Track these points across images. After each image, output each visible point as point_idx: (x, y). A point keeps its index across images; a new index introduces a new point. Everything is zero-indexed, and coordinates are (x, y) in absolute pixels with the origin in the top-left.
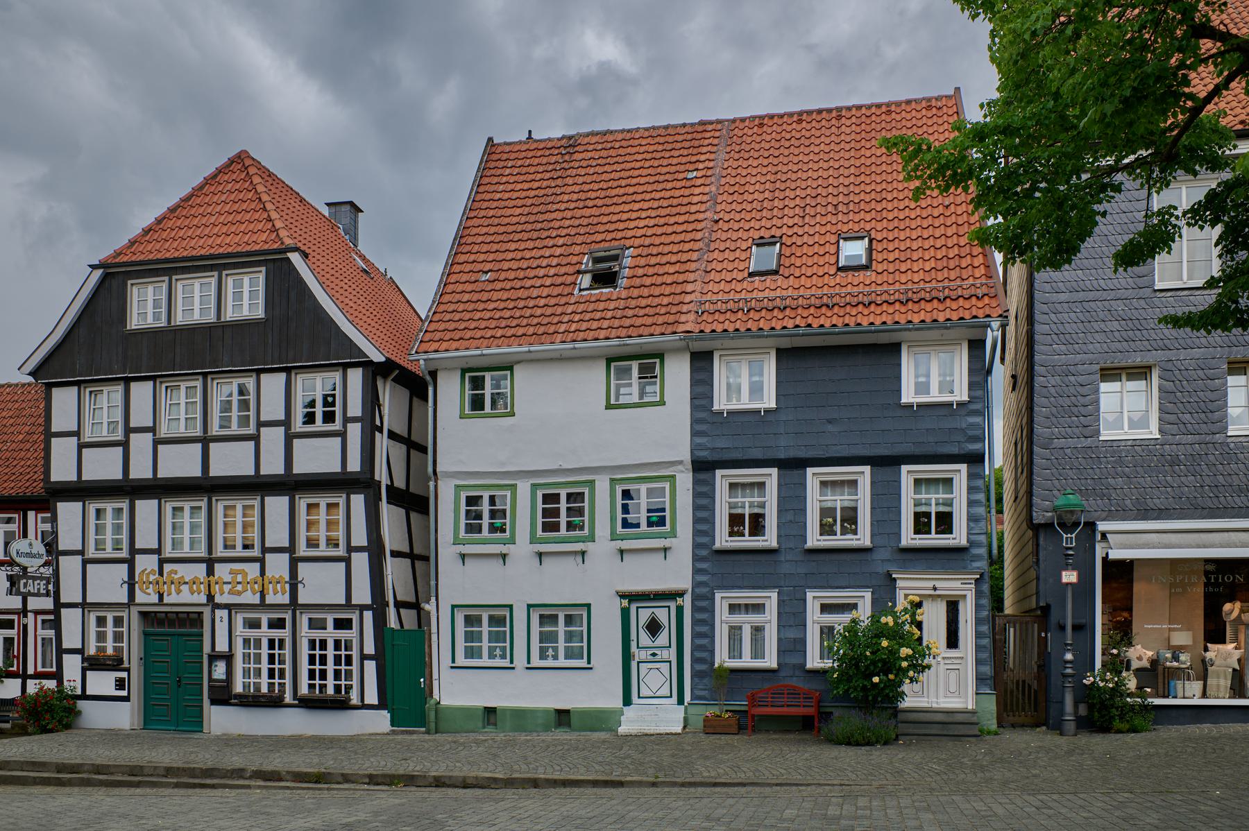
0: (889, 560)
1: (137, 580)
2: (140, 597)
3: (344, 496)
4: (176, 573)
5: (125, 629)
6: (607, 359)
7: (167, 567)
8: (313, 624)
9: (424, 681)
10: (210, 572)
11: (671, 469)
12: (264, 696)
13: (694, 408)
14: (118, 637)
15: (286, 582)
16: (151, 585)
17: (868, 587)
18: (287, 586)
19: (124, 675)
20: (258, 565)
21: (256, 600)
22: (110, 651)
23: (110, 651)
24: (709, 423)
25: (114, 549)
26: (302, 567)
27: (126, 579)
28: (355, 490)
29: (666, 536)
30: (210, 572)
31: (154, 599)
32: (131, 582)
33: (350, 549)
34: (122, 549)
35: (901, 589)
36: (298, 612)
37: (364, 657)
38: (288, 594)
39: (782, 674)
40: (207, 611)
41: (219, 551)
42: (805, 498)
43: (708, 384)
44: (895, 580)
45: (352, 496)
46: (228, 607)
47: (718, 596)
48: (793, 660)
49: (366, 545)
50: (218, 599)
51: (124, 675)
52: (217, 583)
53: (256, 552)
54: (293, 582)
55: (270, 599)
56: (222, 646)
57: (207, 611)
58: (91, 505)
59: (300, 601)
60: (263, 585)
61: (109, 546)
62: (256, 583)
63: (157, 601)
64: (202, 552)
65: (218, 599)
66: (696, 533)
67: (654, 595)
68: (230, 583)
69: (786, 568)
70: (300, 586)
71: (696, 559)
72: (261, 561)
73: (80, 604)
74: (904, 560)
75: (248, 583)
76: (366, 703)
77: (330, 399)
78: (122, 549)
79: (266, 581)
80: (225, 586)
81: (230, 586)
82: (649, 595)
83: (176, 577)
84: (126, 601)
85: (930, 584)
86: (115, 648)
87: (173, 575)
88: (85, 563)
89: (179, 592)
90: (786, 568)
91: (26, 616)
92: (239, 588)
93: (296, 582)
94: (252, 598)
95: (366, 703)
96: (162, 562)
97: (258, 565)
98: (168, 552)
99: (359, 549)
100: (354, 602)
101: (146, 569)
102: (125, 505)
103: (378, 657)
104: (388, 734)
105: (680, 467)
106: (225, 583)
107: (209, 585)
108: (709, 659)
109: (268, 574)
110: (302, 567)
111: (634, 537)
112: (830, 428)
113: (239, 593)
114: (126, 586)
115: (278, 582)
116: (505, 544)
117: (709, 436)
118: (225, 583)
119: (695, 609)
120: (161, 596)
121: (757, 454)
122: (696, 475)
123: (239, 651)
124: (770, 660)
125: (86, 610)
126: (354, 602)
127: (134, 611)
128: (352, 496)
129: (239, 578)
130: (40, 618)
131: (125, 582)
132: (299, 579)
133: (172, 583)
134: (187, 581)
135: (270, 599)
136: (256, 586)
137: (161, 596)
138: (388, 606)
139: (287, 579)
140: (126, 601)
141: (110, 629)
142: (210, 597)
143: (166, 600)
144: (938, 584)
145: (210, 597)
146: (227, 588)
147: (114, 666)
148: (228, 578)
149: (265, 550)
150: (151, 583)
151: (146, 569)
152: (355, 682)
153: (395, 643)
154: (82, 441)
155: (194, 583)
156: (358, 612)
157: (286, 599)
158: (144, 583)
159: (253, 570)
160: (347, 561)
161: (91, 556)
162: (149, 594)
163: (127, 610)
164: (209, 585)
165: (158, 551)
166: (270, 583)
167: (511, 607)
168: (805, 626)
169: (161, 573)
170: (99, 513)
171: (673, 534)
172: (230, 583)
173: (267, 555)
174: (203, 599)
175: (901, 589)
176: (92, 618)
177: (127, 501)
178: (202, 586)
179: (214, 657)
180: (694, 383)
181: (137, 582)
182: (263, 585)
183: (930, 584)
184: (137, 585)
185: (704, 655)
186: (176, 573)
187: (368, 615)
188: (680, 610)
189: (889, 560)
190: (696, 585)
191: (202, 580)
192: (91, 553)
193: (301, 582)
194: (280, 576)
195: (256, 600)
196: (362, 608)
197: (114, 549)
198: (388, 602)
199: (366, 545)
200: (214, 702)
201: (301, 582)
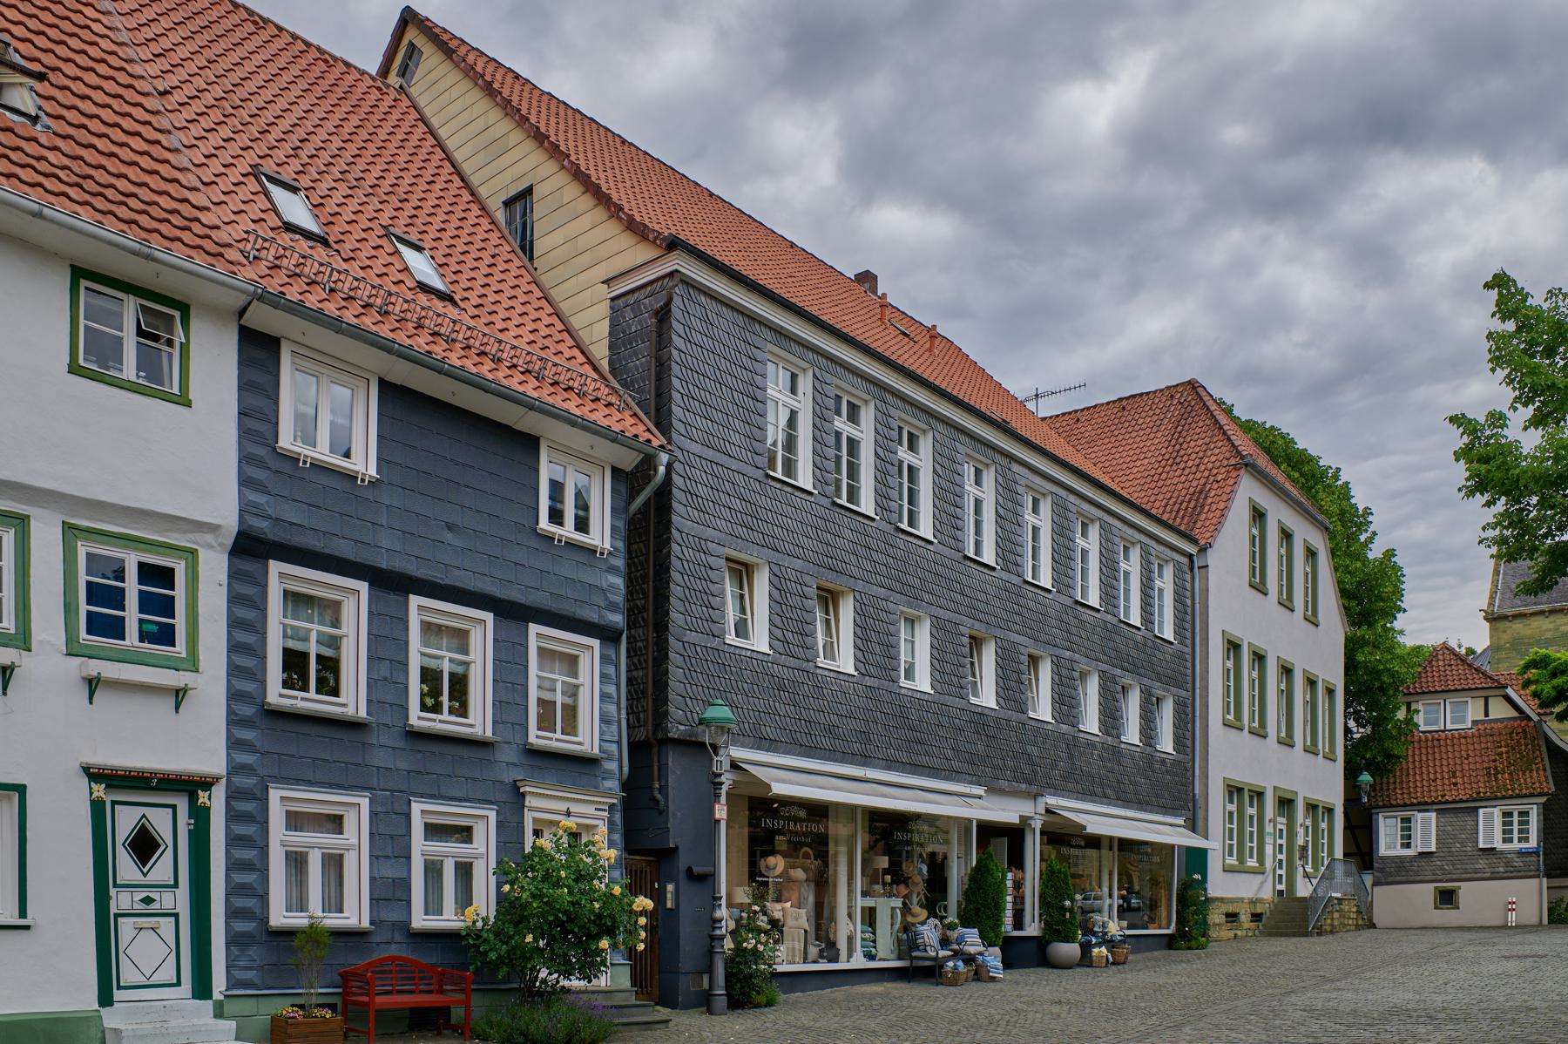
0: (514, 765)
6: (72, 266)
11: (190, 536)
13: (245, 434)
17: (492, 803)
24: (269, 468)
29: (178, 665)
35: (531, 809)
39: (376, 938)
42: (407, 643)
43: (269, 397)
44: (523, 795)
47: (275, 795)
48: (393, 915)
66: (234, 671)
67: (161, 780)
69: (379, 758)
71: (233, 720)
74: (532, 767)
82: (148, 780)
85: (562, 806)
90: (379, 758)
105: (209, 538)
108: (258, 911)
111: (116, 656)
112: (448, 536)
117: (268, 493)
119: (232, 816)
121: (345, 550)
122: (237, 561)
124: (355, 914)
144: (574, 808)
168: (409, 858)
171: (192, 663)
175: (531, 809)
180: (245, 386)
183: (562, 806)
185: (250, 903)
188: (200, 816)
189: (514, 765)
190: (234, 769)
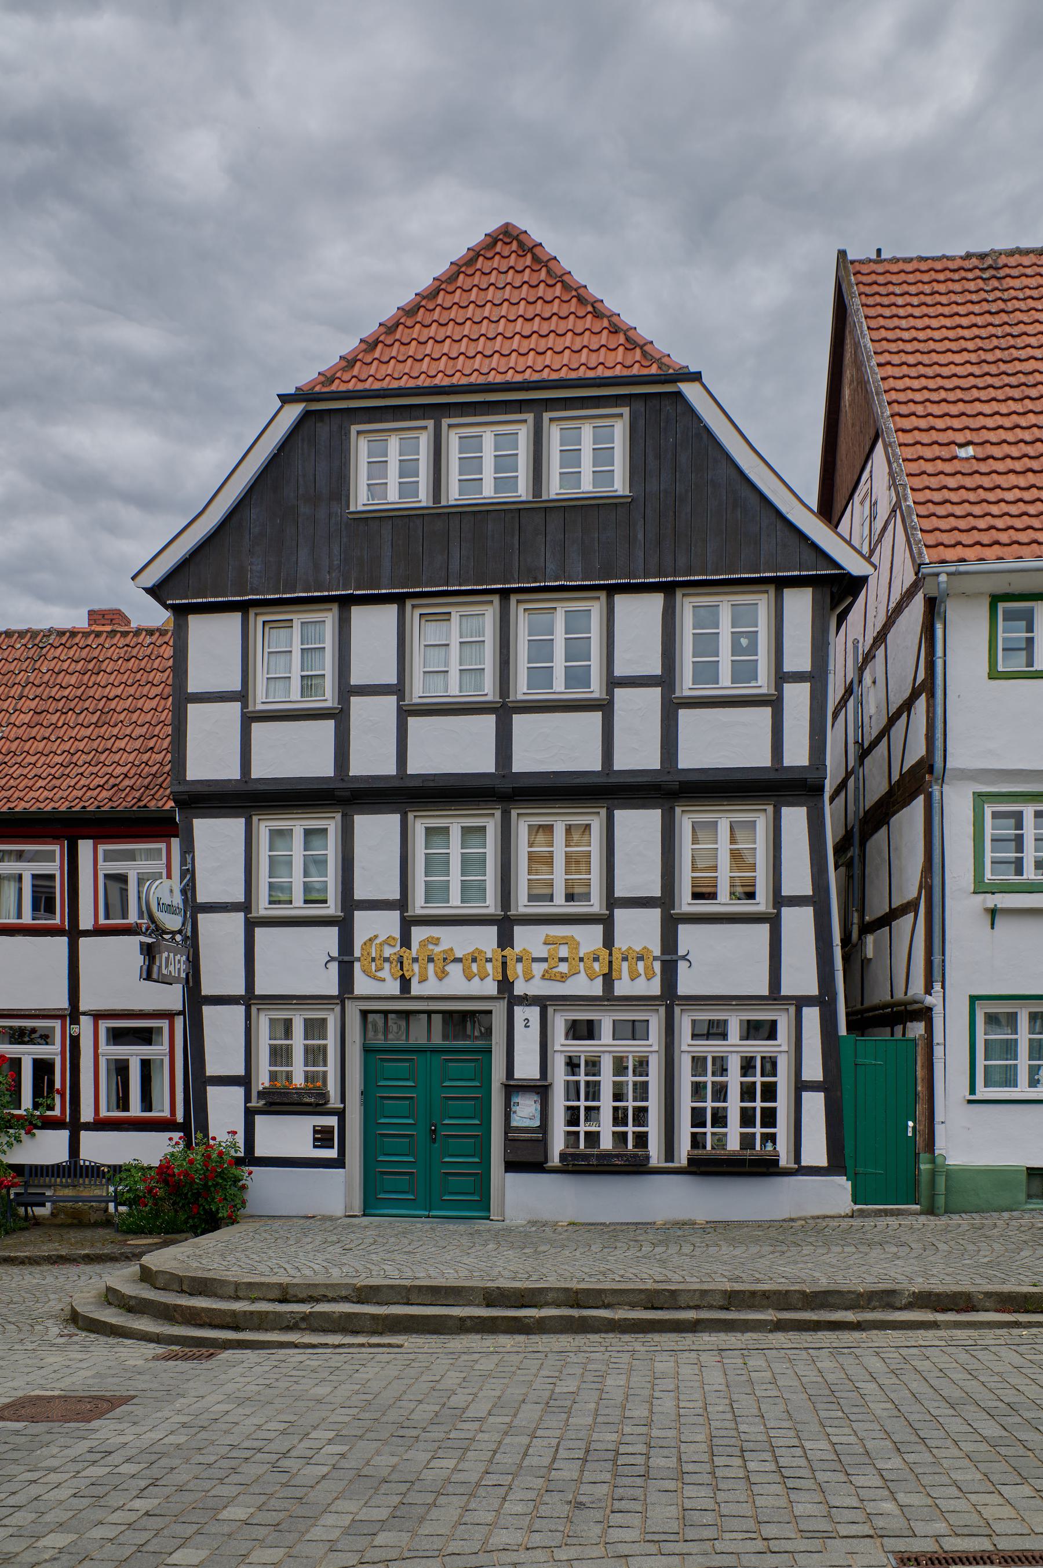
1: (357, 953)
2: (362, 985)
3: (770, 809)
4: (436, 941)
5: (331, 1042)
7: (419, 934)
9: (914, 1128)
10: (505, 940)
12: (606, 1155)
14: (315, 1055)
15: (655, 958)
16: (387, 965)
18: (657, 966)
19: (332, 1121)
20: (599, 929)
21: (596, 988)
22: (299, 1080)
23: (299, 1080)
25: (306, 902)
26: (684, 931)
27: (335, 953)
28: (790, 799)
30: (505, 940)
31: (393, 988)
32: (346, 958)
33: (780, 900)
34: (325, 902)
37: (801, 1087)
40: (499, 1010)
41: (522, 905)
45: (785, 811)
46: (543, 1003)
49: (811, 893)
50: (520, 989)
51: (332, 1121)
52: (519, 960)
53: (596, 905)
54: (667, 958)
55: (622, 988)
57: (499, 1010)
58: (263, 824)
59: (682, 990)
60: (610, 962)
61: (298, 896)
62: (596, 959)
63: (396, 991)
64: (491, 905)
65: (520, 988)
68: (545, 960)
70: (682, 965)
72: (607, 922)
73: (241, 997)
75: (581, 959)
76: (803, 1164)
77: (744, 642)
78: (325, 902)
80: (535, 965)
81: (544, 966)
83: (437, 949)
84: (335, 992)
86: (308, 1077)
87: (431, 947)
88: (251, 926)
89: (442, 975)
91: (75, 1021)
92: (563, 968)
93: (674, 957)
95: (803, 1164)
96: (407, 924)
97: (599, 929)
98: (419, 906)
99: (796, 901)
100: (785, 991)
101: (376, 937)
102: (332, 824)
103: (830, 1086)
104: (846, 1216)
106: (535, 960)
107: (504, 964)
109: (621, 943)
110: (684, 931)
113: (563, 978)
114: (334, 966)
115: (641, 958)
118: (535, 960)
120: (405, 983)
123: (559, 1076)
125: (254, 1009)
126: (785, 991)
127: (353, 1010)
128: (785, 811)
129: (564, 952)
130: (104, 1025)
131: (332, 959)
132: (681, 952)
133: (431, 960)
134: (459, 955)
135: (622, 988)
136: (596, 965)
137: (405, 983)
139: (657, 952)
140: (335, 992)
141: (298, 1042)
142: (505, 985)
143: (416, 989)
145: (505, 985)
146: (538, 969)
147: (318, 1105)
148: (542, 952)
149: (612, 902)
150: (386, 960)
151: (376, 937)
152: (782, 1129)
153: (859, 1061)
154: (251, 709)
155: (474, 960)
156: (792, 1009)
157: (654, 988)
158: (373, 959)
160: (774, 922)
161: (262, 912)
162: (384, 980)
163: (338, 1009)
164: (504, 964)
165: (402, 904)
166: (625, 959)
169: (406, 941)
170: (277, 835)
172: (545, 960)
173: (618, 913)
174: (490, 988)
176: (263, 1023)
177: (338, 816)
178: (489, 966)
179: (513, 1089)
181: (359, 959)
182: (610, 962)
184: (357, 966)
186: (436, 941)
187: (812, 1016)
191: (489, 955)
192: (262, 907)
193: (684, 958)
194: (645, 948)
195: (596, 988)
196: (801, 1002)
197: (306, 902)
199: (811, 893)
200: (511, 1166)
201: (684, 958)
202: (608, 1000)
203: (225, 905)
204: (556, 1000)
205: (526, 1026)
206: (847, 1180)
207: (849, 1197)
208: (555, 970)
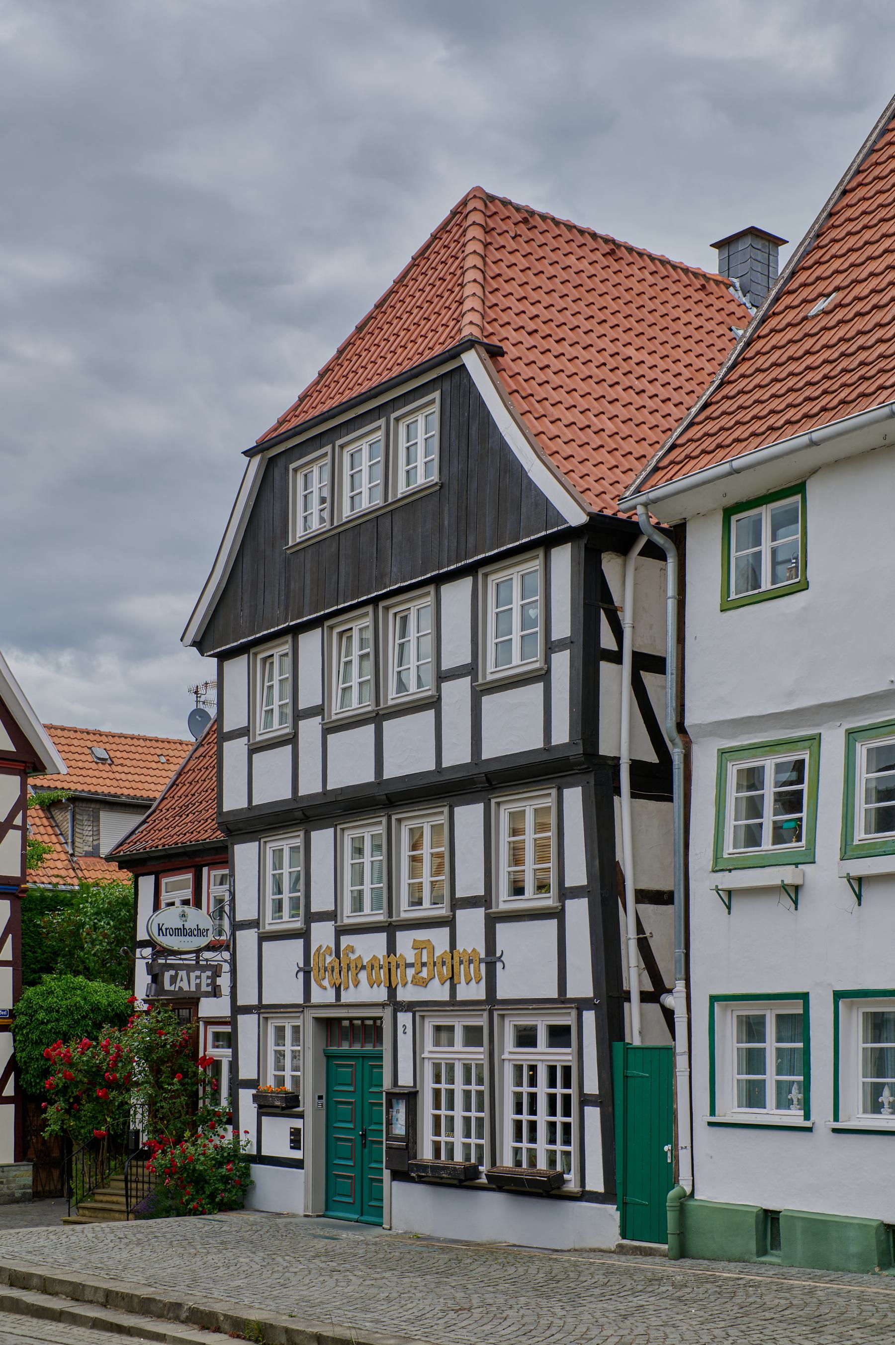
8: (526, 1038)
15: (481, 961)
18: (483, 967)
36: (495, 1013)
38: (483, 982)
56: (405, 1079)
60: (453, 966)
70: (499, 966)
79: (456, 959)
94: (438, 992)
100: (570, 994)
116: (796, 865)
123: (428, 1086)
126: (570, 994)
138: (628, 1000)
139: (483, 955)
159: (439, 938)
160: (558, 914)
167: (804, 997)
174: (381, 994)
182: (453, 966)
196: (581, 1005)
198: (629, 992)
202: (453, 1005)
203: (248, 923)
204: (427, 1006)
205: (405, 1033)
206: (617, 1209)
207: (617, 1230)
208: (420, 975)
